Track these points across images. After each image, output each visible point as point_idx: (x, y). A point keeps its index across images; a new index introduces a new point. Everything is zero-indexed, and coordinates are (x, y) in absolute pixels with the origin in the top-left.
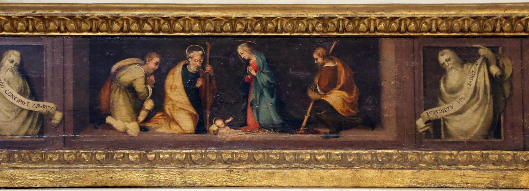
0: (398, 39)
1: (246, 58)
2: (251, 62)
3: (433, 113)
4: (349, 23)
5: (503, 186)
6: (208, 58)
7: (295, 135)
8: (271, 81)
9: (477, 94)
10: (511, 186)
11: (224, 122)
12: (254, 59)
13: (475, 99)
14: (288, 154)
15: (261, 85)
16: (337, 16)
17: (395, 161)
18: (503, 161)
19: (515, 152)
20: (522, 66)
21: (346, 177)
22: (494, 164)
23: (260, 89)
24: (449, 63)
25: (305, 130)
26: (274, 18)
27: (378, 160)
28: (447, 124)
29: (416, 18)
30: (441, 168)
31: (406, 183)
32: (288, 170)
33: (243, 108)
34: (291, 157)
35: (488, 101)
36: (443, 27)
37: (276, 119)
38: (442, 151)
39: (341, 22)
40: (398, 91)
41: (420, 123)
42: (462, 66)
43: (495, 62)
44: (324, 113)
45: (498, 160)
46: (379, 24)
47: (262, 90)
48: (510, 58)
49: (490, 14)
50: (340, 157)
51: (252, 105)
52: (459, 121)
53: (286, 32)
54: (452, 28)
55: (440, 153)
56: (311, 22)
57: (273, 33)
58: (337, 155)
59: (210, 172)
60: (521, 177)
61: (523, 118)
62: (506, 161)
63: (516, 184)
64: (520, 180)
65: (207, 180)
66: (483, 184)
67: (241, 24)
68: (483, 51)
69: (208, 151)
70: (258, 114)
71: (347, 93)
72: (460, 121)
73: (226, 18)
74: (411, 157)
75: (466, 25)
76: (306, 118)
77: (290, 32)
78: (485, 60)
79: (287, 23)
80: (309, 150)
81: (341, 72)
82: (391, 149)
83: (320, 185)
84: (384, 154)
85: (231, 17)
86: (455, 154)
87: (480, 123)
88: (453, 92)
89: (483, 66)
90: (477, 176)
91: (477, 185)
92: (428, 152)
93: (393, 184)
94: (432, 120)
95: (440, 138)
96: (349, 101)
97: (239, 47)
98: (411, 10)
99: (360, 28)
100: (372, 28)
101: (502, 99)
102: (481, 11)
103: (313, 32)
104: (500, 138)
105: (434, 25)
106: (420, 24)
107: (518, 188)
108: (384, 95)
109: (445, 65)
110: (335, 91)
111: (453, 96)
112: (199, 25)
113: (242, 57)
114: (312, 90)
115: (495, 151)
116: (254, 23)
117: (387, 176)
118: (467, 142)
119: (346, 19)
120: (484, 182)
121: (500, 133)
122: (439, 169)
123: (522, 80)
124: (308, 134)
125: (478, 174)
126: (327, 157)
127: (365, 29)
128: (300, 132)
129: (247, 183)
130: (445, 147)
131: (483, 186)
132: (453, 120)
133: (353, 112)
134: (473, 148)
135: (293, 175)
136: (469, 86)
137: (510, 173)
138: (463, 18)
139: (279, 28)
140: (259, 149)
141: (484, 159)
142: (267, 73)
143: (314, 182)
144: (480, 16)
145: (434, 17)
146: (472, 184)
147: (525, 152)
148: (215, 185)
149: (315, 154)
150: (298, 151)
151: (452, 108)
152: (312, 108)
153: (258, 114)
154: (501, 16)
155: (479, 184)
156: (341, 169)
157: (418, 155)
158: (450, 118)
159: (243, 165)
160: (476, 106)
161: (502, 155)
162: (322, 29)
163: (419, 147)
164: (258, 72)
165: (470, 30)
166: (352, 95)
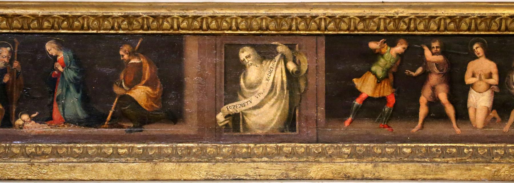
0: (202, 36)
1: (54, 55)
2: (59, 58)
3: (232, 107)
4: (153, 21)
5: (294, 178)
6: (16, 54)
7: (99, 129)
8: (78, 77)
9: (274, 89)
10: (301, 177)
11: (30, 116)
12: (61, 55)
14: (91, 148)
15: (67, 81)
16: (141, 14)
17: (195, 155)
18: (296, 153)
19: (308, 145)
20: (317, 63)
21: (145, 170)
22: (287, 157)
23: (66, 85)
24: (249, 59)
25: (109, 124)
26: (79, 16)
27: (178, 153)
28: (246, 118)
29: (217, 17)
30: (237, 160)
32: (89, 164)
33: (49, 102)
34: (94, 150)
35: (285, 96)
37: (81, 114)
38: (240, 144)
39: (145, 20)
40: (200, 87)
41: (220, 117)
42: (261, 63)
43: (292, 59)
44: (128, 108)
45: (291, 153)
46: (182, 22)
47: (68, 85)
48: (306, 55)
49: (286, 14)
50: (141, 150)
51: (58, 100)
53: (93, 30)
54: (251, 27)
55: (238, 146)
56: (116, 20)
57: (80, 30)
58: (139, 149)
59: (12, 165)
60: (311, 169)
61: (317, 112)
62: (299, 153)
63: (306, 175)
64: (310, 171)
65: (8, 173)
67: (49, 21)
68: (281, 49)
69: (12, 144)
70: (63, 109)
71: (151, 88)
72: (258, 114)
73: (33, 15)
74: (210, 150)
75: (264, 24)
76: (111, 112)
77: (97, 29)
78: (283, 57)
79: (93, 21)
80: (113, 144)
81: (146, 69)
82: (192, 142)
83: (120, 179)
84: (184, 148)
85: (38, 15)
86: (252, 147)
87: (277, 117)
88: (251, 87)
89: (280, 63)
90: (269, 168)
91: (269, 177)
93: (190, 177)
94: (231, 114)
95: (239, 131)
96: (153, 96)
97: (47, 44)
98: (223, 8)
99: (164, 26)
100: (175, 26)
101: (298, 93)
103: (119, 30)
104: (295, 131)
105: (234, 24)
106: (221, 22)
107: (307, 180)
108: (186, 91)
109: (245, 61)
110: (139, 86)
111: (252, 91)
112: (6, 22)
113: (50, 53)
114: (117, 85)
116: (61, 21)
117: (184, 169)
118: (264, 135)
119: (150, 17)
120: (276, 173)
121: (295, 126)
122: (235, 162)
123: (316, 76)
124: (112, 128)
126: (129, 150)
127: (169, 27)
128: (105, 126)
129: (48, 176)
130: (243, 140)
131: (275, 178)
132: (251, 114)
133: (157, 106)
134: (269, 141)
135: (93, 168)
137: (300, 165)
138: (261, 17)
139: (85, 26)
140: (63, 143)
142: (74, 69)
143: (114, 175)
144: (276, 15)
146: (264, 176)
148: (16, 178)
149: (117, 148)
150: (102, 145)
151: (251, 102)
152: (117, 103)
153: (63, 109)
154: (296, 15)
155: (271, 176)
156: (140, 162)
157: (217, 148)
159: (45, 158)
160: (273, 100)
161: (296, 147)
162: (127, 27)
163: (218, 141)
164: (65, 68)
165: (267, 29)
166: (156, 91)
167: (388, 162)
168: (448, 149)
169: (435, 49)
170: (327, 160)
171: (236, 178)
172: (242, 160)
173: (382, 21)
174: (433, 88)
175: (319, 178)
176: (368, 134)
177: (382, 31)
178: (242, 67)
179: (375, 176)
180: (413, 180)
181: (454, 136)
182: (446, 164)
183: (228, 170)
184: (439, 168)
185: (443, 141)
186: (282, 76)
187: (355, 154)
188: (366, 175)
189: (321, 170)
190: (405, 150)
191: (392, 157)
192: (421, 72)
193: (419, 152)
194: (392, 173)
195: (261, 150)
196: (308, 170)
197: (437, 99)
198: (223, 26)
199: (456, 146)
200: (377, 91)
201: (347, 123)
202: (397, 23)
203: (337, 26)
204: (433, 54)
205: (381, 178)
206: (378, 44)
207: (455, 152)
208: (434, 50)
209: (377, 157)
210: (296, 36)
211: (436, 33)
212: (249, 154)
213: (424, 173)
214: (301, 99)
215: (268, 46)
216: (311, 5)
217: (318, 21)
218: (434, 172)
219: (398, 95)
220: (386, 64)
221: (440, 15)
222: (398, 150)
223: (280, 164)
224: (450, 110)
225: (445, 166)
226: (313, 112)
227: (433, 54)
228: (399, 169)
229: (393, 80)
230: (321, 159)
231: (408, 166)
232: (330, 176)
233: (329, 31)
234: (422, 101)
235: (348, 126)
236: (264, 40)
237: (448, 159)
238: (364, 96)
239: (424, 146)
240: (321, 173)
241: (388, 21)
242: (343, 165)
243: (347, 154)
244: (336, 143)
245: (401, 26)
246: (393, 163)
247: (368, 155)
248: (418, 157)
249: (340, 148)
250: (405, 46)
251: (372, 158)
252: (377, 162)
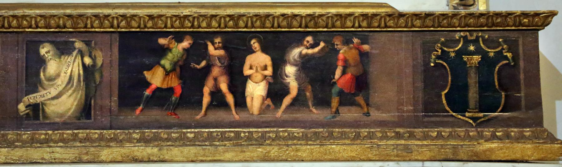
0: (5, 34)
3: (33, 98)
5: (86, 161)
9: (72, 81)
10: (93, 160)
13: (70, 86)
18: (90, 139)
19: (102, 131)
20: (111, 57)
22: (81, 142)
30: (34, 146)
31: (2, 160)
35: (81, 88)
36: (42, 24)
38: (39, 131)
41: (22, 107)
42: (60, 58)
43: (88, 54)
48: (101, 50)
52: (55, 105)
55: (37, 133)
60: (102, 153)
61: (110, 102)
62: (92, 138)
64: (101, 155)
66: (69, 159)
74: (11, 137)
75: (61, 22)
78: (80, 53)
86: (50, 134)
87: (74, 107)
89: (78, 57)
91: (63, 160)
92: (26, 132)
94: (31, 104)
95: (39, 120)
102: (93, 9)
104: (90, 119)
105: (33, 22)
109: (45, 56)
111: (51, 83)
115: (84, 131)
118: (61, 123)
120: (70, 157)
121: (91, 114)
122: (32, 147)
123: (110, 69)
125: (64, 151)
130: (42, 128)
131: (69, 161)
132: (50, 104)
136: (65, 74)
137: (92, 149)
138: (58, 16)
141: (74, 138)
145: (33, 15)
146: (59, 159)
147: (110, 131)
151: (50, 93)
154: (90, 14)
155: (65, 159)
158: (48, 102)
160: (70, 92)
161: (90, 134)
165: (65, 27)
167: (172, 146)
168: (227, 134)
169: (218, 44)
170: (117, 145)
171: (33, 161)
172: (39, 145)
173: (169, 19)
174: (215, 79)
175: (110, 161)
176: (157, 121)
177: (169, 28)
178: (42, 62)
179: (160, 158)
180: (192, 161)
181: (233, 122)
182: (223, 147)
183: (25, 155)
184: (217, 150)
185: (224, 126)
186: (79, 70)
187: (143, 139)
188: (152, 158)
189: (111, 154)
190: (189, 135)
191: (176, 141)
192: (204, 66)
193: (201, 136)
194: (175, 155)
195: (58, 136)
196: (99, 153)
197: (219, 89)
198: (23, 24)
199: (235, 130)
200: (166, 83)
201: (138, 112)
202: (182, 21)
203: (128, 24)
204: (216, 49)
205: (165, 160)
206: (166, 40)
207: (233, 136)
208: (216, 46)
209: (163, 141)
210: (92, 33)
211: (218, 30)
212: (46, 140)
213: (204, 155)
214: (96, 90)
215: (66, 43)
216: (114, 6)
217: (111, 20)
218: (213, 154)
219: (184, 85)
220: (174, 58)
221: (220, 13)
222: (183, 135)
223: (74, 149)
224: (230, 99)
225: (222, 149)
226: (107, 102)
227: (216, 49)
228: (181, 152)
229: (179, 73)
230: (111, 144)
231: (190, 149)
232: (120, 159)
233: (122, 28)
234: (205, 91)
235: (138, 114)
236: (62, 37)
237: (226, 143)
238: (153, 87)
239: (206, 132)
240: (111, 157)
241: (174, 19)
242: (131, 149)
243: (136, 139)
244: (128, 129)
245: (186, 23)
246: (176, 146)
247: (156, 140)
248: (199, 141)
249: (131, 134)
250: (191, 42)
251: (158, 142)
252: (162, 146)
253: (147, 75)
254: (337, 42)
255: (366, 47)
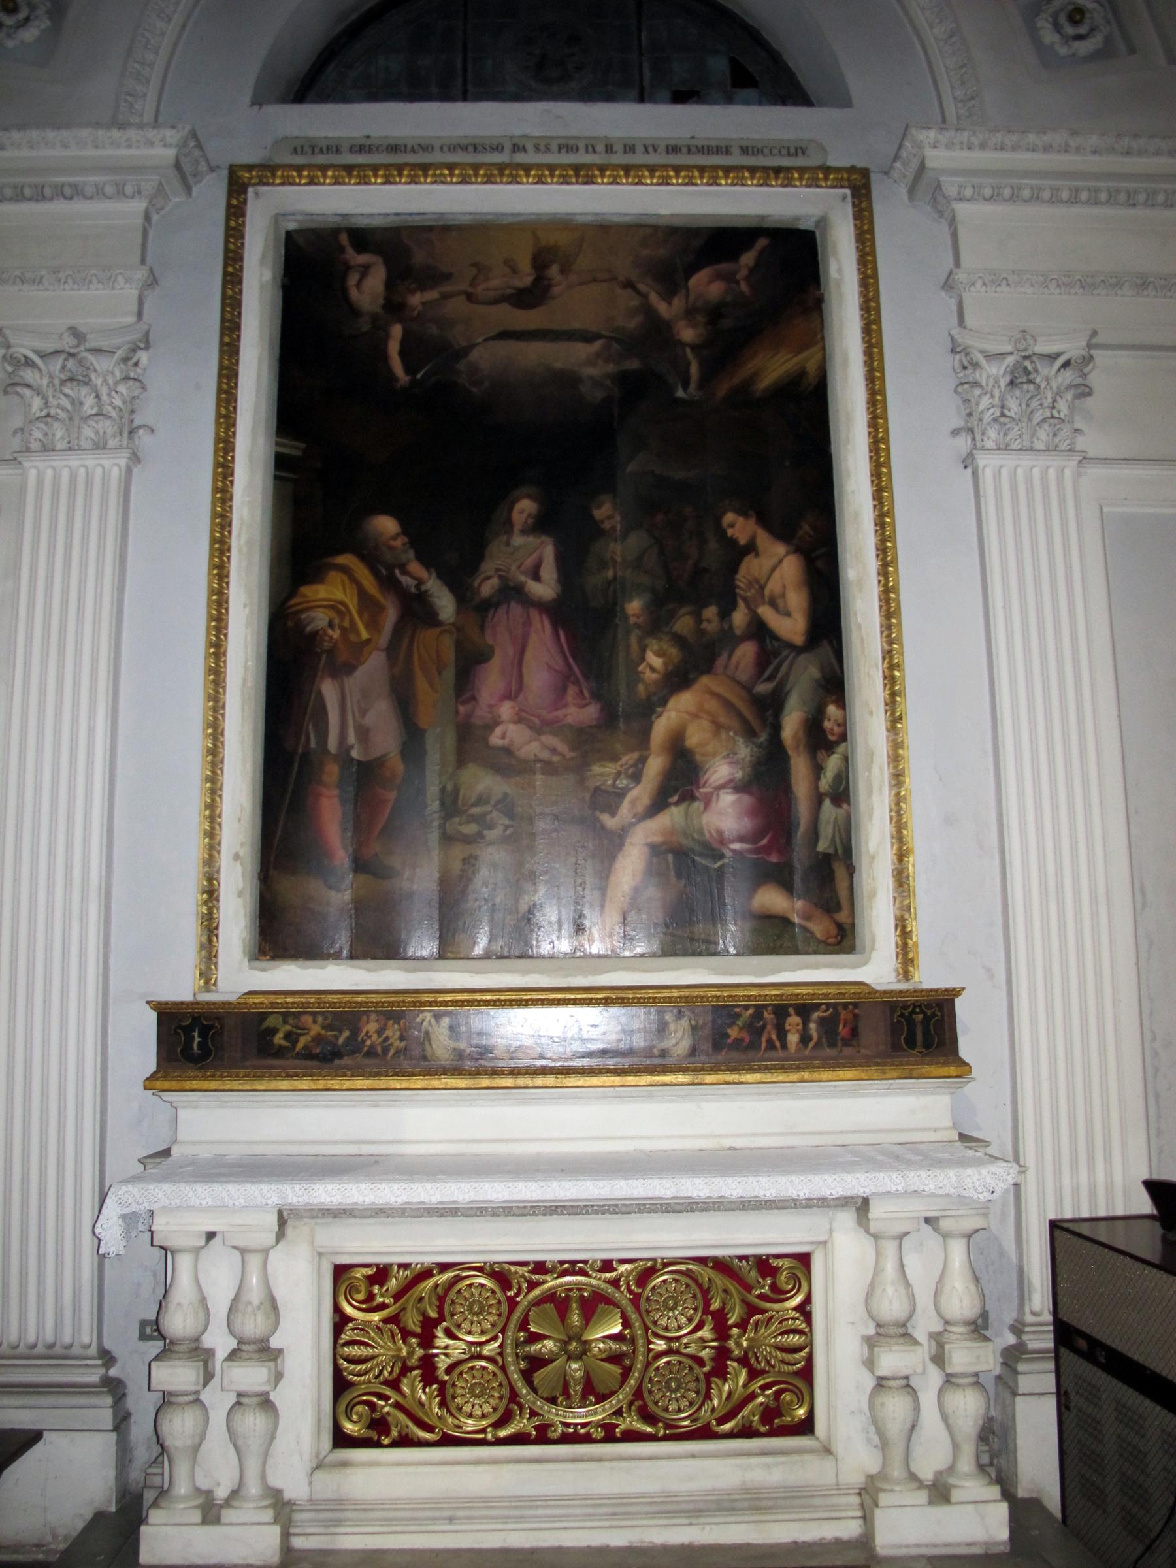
224: (778, 1044)
253: (729, 1031)
254: (840, 1008)
255: (857, 1011)
